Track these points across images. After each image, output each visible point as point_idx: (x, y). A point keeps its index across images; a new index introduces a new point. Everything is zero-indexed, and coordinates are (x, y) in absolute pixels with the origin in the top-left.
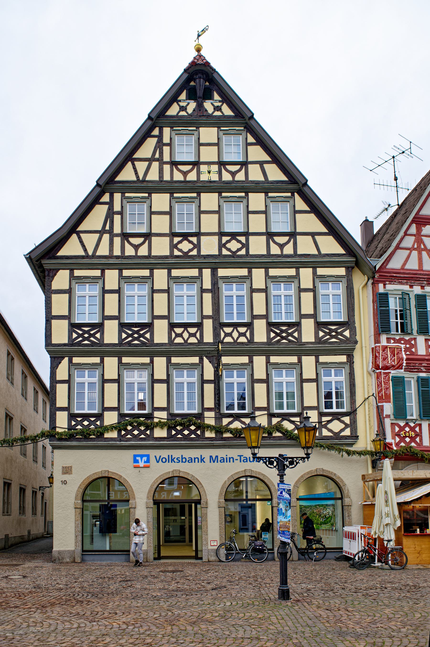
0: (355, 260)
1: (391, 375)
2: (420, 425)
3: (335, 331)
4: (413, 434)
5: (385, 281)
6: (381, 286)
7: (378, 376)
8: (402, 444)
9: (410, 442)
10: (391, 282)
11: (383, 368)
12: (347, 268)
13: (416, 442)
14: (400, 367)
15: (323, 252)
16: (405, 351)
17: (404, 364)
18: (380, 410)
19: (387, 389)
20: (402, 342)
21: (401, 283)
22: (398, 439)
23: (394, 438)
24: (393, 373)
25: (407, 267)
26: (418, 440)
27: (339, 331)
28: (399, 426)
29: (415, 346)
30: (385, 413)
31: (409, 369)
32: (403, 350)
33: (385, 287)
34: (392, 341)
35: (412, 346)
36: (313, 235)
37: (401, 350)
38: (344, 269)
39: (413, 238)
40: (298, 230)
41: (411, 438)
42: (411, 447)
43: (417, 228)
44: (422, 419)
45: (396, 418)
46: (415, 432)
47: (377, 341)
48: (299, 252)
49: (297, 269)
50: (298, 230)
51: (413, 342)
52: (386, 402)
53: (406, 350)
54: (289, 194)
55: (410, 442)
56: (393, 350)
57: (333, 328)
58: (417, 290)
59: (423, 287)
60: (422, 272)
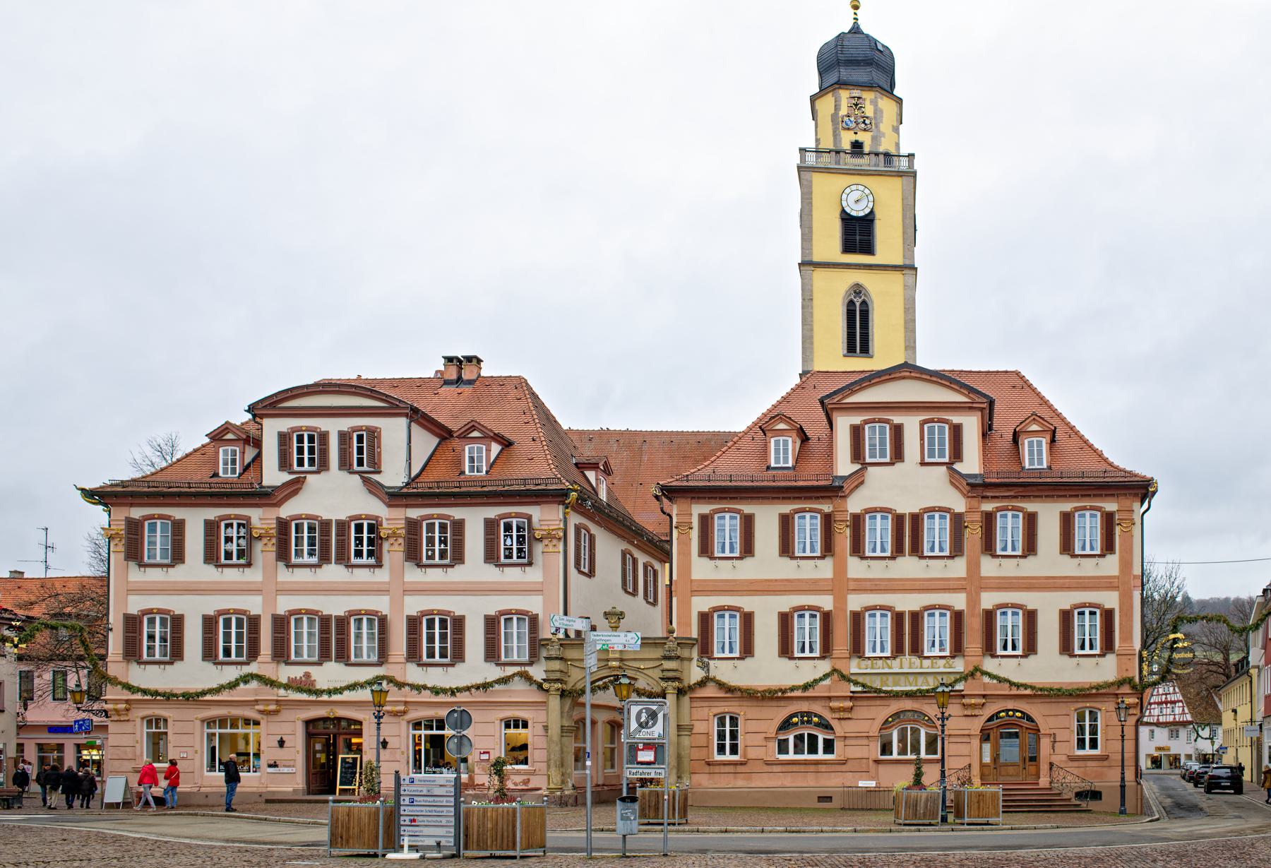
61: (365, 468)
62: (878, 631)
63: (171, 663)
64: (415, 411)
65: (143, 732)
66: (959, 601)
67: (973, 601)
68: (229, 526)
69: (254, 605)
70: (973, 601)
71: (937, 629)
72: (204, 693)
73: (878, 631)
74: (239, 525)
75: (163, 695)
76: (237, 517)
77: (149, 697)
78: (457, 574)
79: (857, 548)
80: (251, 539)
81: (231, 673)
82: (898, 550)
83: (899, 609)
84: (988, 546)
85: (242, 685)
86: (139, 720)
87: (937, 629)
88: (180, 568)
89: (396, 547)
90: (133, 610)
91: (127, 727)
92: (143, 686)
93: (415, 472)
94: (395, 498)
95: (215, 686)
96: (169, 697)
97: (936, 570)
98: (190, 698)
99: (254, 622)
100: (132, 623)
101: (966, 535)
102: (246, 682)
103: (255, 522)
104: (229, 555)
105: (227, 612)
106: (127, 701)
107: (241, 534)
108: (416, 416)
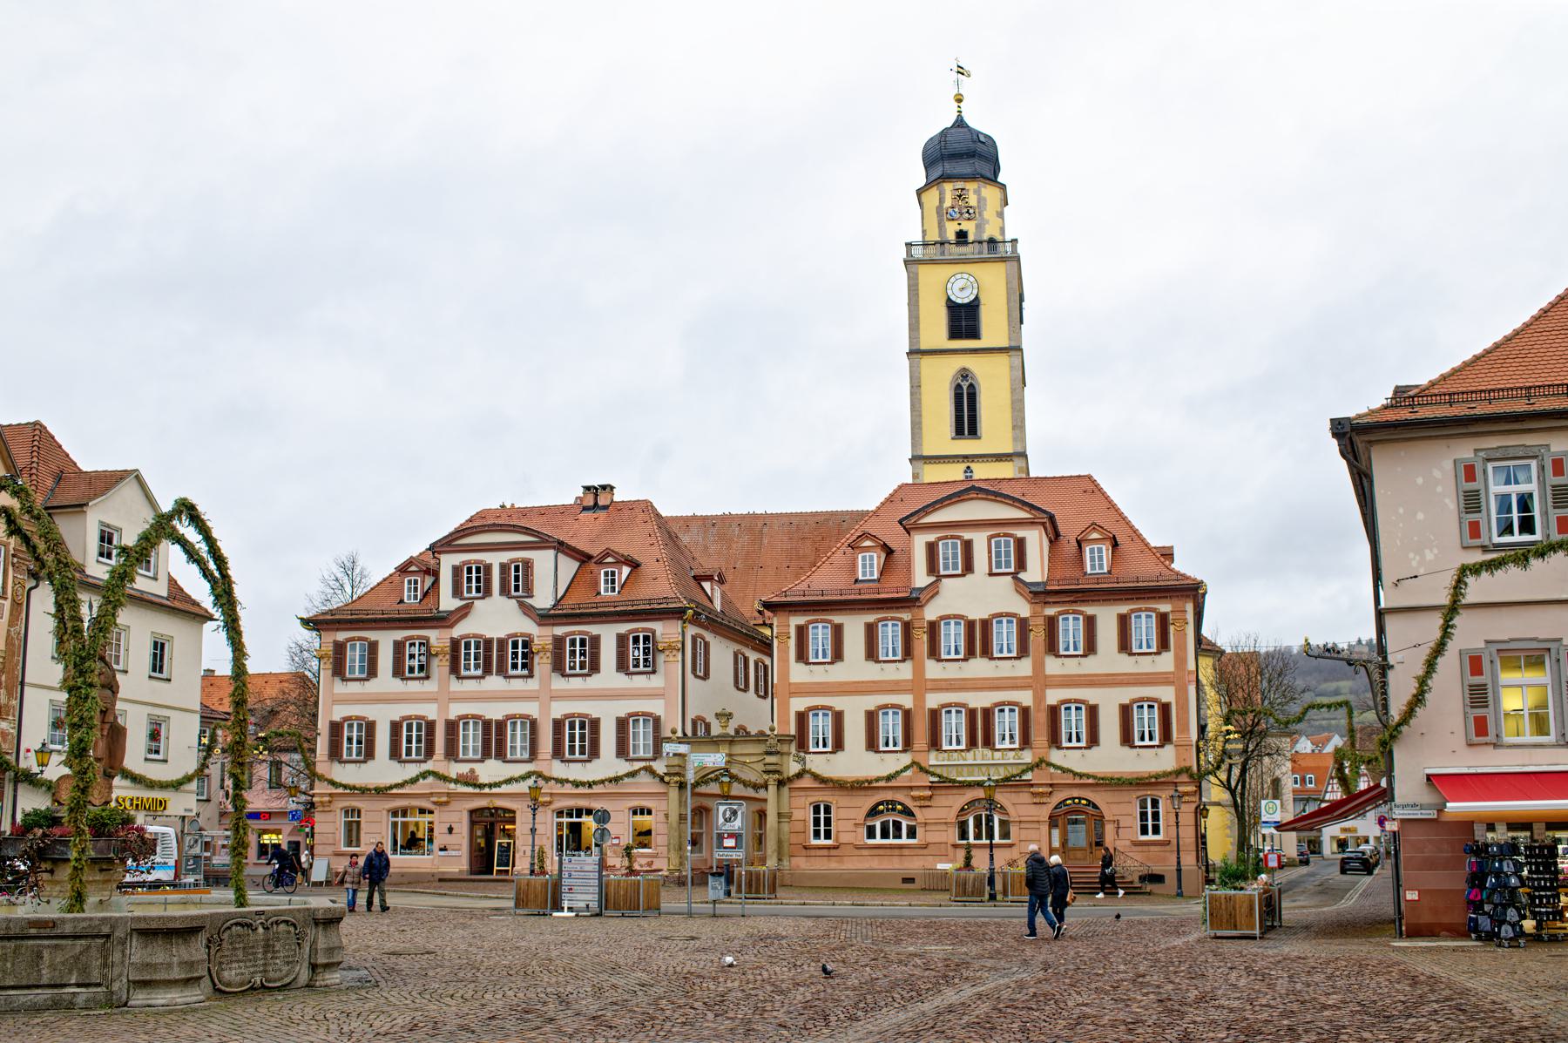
61: (520, 593)
62: (954, 725)
63: (365, 762)
64: (561, 543)
65: (341, 820)
66: (1026, 698)
67: (1040, 697)
68: (413, 645)
69: (430, 711)
70: (1040, 697)
71: (1006, 723)
72: (391, 787)
73: (954, 725)
74: (420, 644)
75: (360, 789)
76: (419, 637)
77: (348, 791)
78: (594, 682)
79: (934, 652)
80: (429, 655)
81: (412, 770)
82: (970, 653)
83: (972, 705)
84: (1052, 647)
85: (421, 780)
86: (338, 811)
87: (1006, 723)
88: (373, 681)
89: (545, 660)
90: (337, 718)
91: (329, 817)
92: (343, 782)
93: (560, 593)
94: (544, 618)
95: (400, 782)
96: (364, 791)
97: (1006, 670)
98: (381, 792)
99: (431, 726)
100: (336, 728)
101: (1031, 638)
102: (424, 778)
103: (433, 641)
104: (411, 670)
105: (409, 718)
106: (330, 795)
107: (422, 652)
108: (562, 547)
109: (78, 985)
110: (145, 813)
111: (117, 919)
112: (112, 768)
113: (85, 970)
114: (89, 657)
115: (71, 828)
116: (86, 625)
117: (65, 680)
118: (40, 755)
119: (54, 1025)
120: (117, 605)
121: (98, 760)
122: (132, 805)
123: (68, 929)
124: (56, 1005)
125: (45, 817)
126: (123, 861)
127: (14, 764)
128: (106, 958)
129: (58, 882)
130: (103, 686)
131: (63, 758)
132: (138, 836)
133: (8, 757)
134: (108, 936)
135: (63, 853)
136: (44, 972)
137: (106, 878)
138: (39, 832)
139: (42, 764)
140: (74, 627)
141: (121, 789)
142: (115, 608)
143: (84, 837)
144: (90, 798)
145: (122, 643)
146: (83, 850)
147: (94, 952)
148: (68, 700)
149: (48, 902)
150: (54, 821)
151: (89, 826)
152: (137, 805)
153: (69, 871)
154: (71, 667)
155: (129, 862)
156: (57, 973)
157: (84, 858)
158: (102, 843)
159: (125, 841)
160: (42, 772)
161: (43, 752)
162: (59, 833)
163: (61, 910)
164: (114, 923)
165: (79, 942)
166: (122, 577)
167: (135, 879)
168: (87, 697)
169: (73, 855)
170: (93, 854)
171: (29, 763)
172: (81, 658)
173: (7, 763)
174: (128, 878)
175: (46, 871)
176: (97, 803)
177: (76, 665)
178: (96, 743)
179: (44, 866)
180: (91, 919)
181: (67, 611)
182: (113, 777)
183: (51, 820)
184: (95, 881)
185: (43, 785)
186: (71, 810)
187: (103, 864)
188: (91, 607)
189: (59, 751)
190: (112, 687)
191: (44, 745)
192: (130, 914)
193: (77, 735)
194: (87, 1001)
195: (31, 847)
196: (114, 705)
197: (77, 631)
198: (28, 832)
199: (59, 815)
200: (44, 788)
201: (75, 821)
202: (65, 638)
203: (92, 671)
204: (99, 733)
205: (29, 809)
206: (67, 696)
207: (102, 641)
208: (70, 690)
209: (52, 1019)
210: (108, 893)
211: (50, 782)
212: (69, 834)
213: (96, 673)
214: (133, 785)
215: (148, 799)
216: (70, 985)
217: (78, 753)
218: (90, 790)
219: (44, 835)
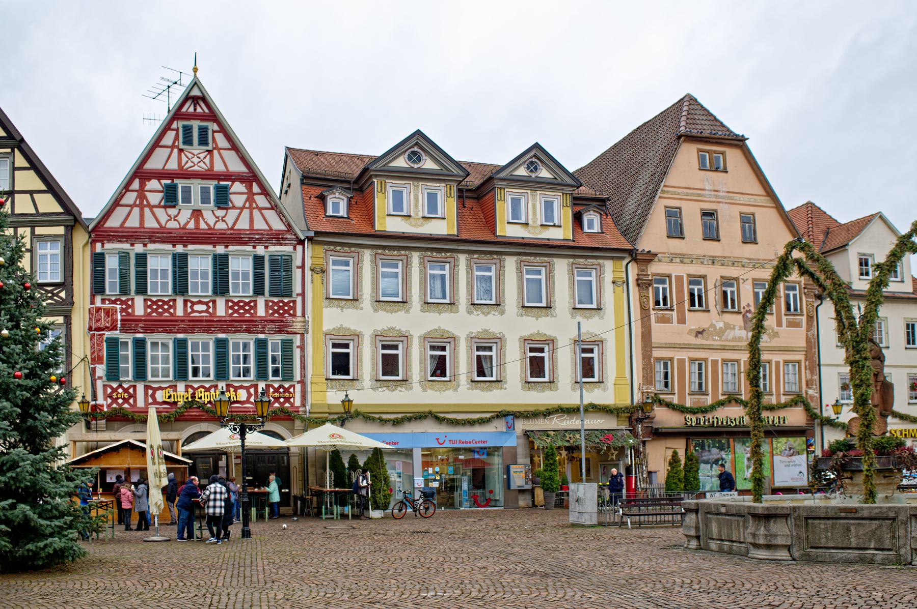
0: (73, 218)
1: (105, 337)
2: (135, 387)
3: (51, 292)
4: (126, 396)
5: (103, 241)
6: (99, 245)
7: (92, 337)
8: (114, 406)
9: (123, 404)
10: (109, 241)
11: (96, 330)
12: (66, 227)
13: (129, 404)
14: (114, 328)
15: (41, 211)
16: (121, 312)
17: (119, 326)
18: (93, 372)
19: (100, 350)
20: (118, 303)
21: (121, 242)
22: (109, 401)
23: (105, 399)
24: (107, 334)
25: (127, 225)
26: (131, 401)
27: (55, 292)
28: (111, 387)
29: (132, 306)
30: (98, 374)
31: (125, 330)
32: (119, 310)
33: (103, 246)
34: (107, 302)
35: (129, 307)
36: (31, 193)
37: (116, 312)
38: (63, 228)
39: (136, 194)
40: (16, 189)
41: (124, 399)
42: (123, 409)
43: (140, 183)
44: (135, 381)
45: (108, 380)
46: (129, 393)
47: (93, 302)
48: (16, 212)
49: (16, 228)
50: (16, 189)
51: (130, 303)
52: (98, 364)
53: (122, 310)
54: (9, 150)
55: (123, 404)
56: (107, 312)
57: (49, 289)
58: (139, 248)
59: (145, 245)
60: (142, 230)
109: (876, 549)
110: (912, 439)
111: (900, 508)
112: (886, 410)
113: (880, 540)
114: (862, 340)
115: (862, 451)
116: (857, 320)
117: (847, 358)
118: (835, 407)
119: (862, 573)
120: (877, 303)
121: (875, 406)
122: (901, 434)
123: (866, 514)
124: (861, 560)
125: (844, 445)
126: (900, 470)
127: (819, 414)
128: (893, 533)
129: (857, 485)
130: (874, 358)
131: (852, 407)
132: (910, 454)
133: (815, 411)
134: (894, 519)
135: (857, 466)
136: (852, 540)
137: (889, 482)
138: (841, 454)
139: (837, 413)
140: (849, 323)
141: (894, 425)
142: (876, 305)
143: (871, 456)
144: (872, 431)
145: (883, 329)
146: (871, 464)
147: (885, 529)
148: (851, 370)
149: (851, 497)
150: (850, 447)
151: (874, 449)
152: (906, 435)
153: (863, 477)
154: (850, 349)
155: (904, 471)
156: (861, 541)
157: (872, 469)
158: (884, 459)
159: (900, 458)
160: (838, 418)
161: (837, 406)
162: (854, 454)
163: (860, 502)
164: (898, 510)
165: (874, 522)
166: (879, 284)
167: (910, 483)
168: (863, 367)
169: (865, 467)
170: (878, 467)
171: (829, 413)
172: (857, 342)
173: (815, 414)
174: (905, 482)
175: (847, 478)
176: (878, 434)
177: (853, 347)
178: (873, 395)
179: (846, 475)
180: (881, 508)
181: (843, 314)
182: (887, 417)
183: (847, 446)
184: (881, 484)
185: (839, 426)
186: (861, 439)
187: (886, 473)
188: (859, 308)
189: (847, 404)
190: (880, 358)
191: (837, 401)
192: (908, 505)
193: (860, 392)
194: (883, 559)
195: (836, 464)
196: (882, 369)
197: (852, 326)
198: (834, 454)
199: (853, 443)
200: (840, 428)
201: (864, 446)
202: (845, 331)
203: (865, 349)
204: (874, 389)
205: (832, 440)
206: (850, 368)
207: (870, 329)
208: (851, 364)
209: (860, 569)
210: (891, 491)
211: (844, 423)
212: (860, 455)
213: (868, 350)
214: (901, 421)
215: (913, 430)
216: (870, 549)
217: (861, 403)
218: (872, 425)
219: (844, 456)
